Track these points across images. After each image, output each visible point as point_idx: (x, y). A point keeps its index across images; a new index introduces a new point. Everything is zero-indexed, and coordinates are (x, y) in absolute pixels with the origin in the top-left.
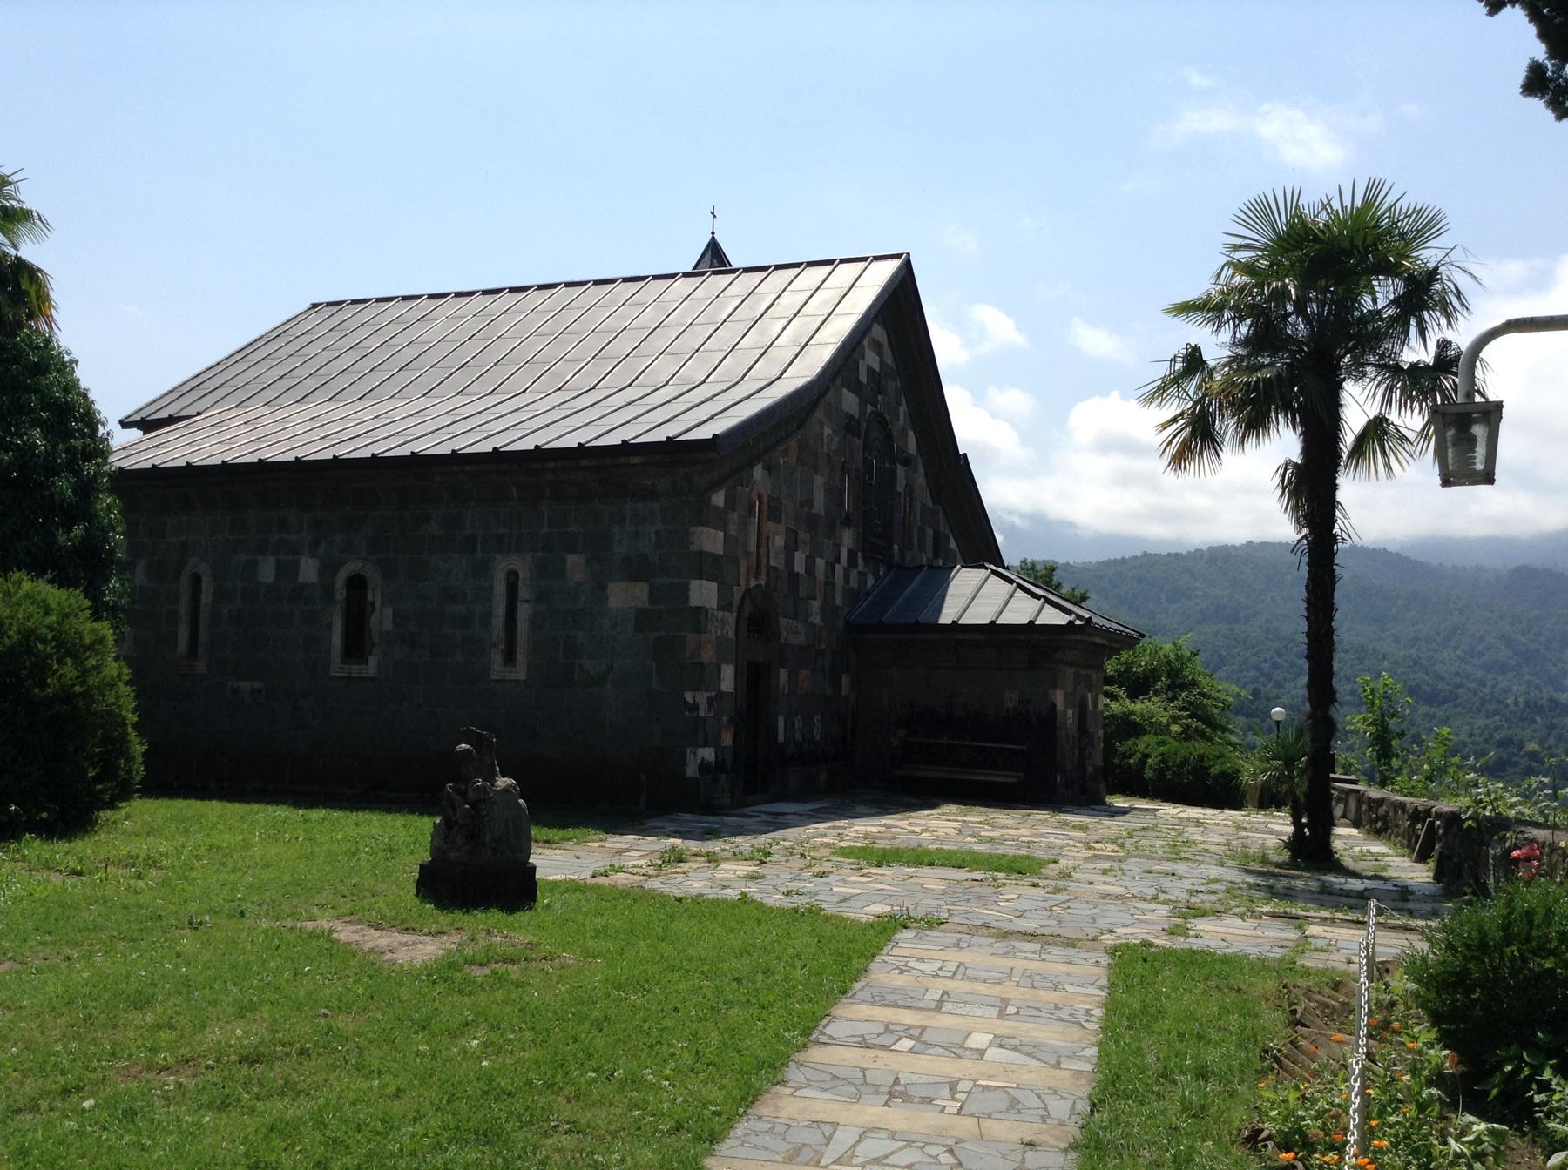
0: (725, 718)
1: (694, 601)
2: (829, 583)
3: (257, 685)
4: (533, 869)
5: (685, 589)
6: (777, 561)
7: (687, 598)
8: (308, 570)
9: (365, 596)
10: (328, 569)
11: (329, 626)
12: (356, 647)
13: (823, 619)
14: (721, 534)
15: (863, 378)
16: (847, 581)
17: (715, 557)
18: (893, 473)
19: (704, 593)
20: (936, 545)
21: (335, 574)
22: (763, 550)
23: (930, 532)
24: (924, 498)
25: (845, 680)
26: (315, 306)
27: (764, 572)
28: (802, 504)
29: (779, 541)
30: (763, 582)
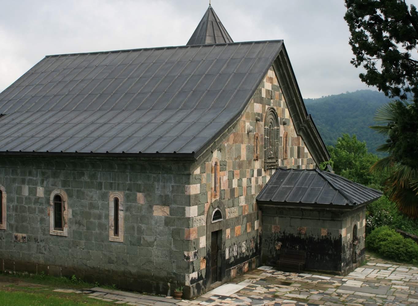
1: (187, 215)
2: (249, 187)
3: (24, 235)
5: (184, 209)
6: (224, 186)
7: (184, 214)
8: (40, 192)
10: (48, 192)
11: (49, 215)
12: (59, 224)
13: (246, 203)
16: (257, 182)
17: (196, 196)
18: (278, 130)
19: (192, 211)
21: (50, 195)
22: (218, 185)
23: (296, 148)
25: (256, 224)
27: (218, 194)
28: (236, 159)
29: (225, 178)
30: (218, 198)
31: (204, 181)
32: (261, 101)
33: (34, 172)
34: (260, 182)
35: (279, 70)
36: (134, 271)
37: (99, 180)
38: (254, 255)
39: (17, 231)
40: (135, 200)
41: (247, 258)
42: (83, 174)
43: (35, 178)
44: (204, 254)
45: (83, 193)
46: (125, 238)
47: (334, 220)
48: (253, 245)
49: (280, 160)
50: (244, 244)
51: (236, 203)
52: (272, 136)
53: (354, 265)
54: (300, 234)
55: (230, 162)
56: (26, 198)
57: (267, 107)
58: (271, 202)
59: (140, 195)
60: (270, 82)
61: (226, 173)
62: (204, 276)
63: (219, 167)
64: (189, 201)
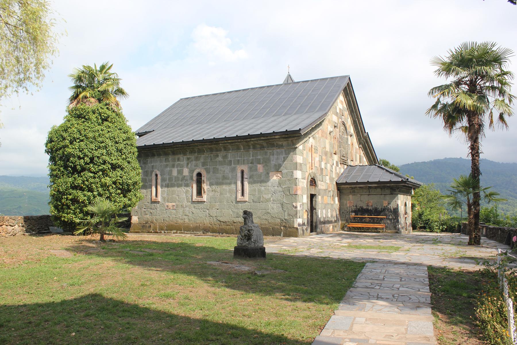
0: (304, 210)
1: (295, 177)
3: (174, 204)
4: (265, 248)
6: (317, 165)
7: (292, 176)
8: (186, 172)
9: (201, 179)
10: (191, 172)
14: (302, 157)
15: (338, 111)
16: (336, 170)
17: (301, 164)
19: (298, 174)
20: (360, 159)
21: (193, 173)
22: (313, 162)
24: (356, 145)
26: (181, 99)
28: (323, 148)
29: (317, 159)
31: (305, 156)
33: (181, 158)
35: (346, 97)
37: (229, 159)
38: (335, 221)
39: (168, 201)
42: (218, 156)
43: (182, 163)
45: (218, 169)
46: (249, 198)
47: (392, 194)
48: (334, 214)
52: (342, 143)
54: (368, 206)
56: (175, 177)
57: (340, 120)
58: (346, 183)
59: (260, 167)
60: (341, 103)
61: (318, 155)
62: (306, 224)
63: (313, 149)
64: (296, 166)
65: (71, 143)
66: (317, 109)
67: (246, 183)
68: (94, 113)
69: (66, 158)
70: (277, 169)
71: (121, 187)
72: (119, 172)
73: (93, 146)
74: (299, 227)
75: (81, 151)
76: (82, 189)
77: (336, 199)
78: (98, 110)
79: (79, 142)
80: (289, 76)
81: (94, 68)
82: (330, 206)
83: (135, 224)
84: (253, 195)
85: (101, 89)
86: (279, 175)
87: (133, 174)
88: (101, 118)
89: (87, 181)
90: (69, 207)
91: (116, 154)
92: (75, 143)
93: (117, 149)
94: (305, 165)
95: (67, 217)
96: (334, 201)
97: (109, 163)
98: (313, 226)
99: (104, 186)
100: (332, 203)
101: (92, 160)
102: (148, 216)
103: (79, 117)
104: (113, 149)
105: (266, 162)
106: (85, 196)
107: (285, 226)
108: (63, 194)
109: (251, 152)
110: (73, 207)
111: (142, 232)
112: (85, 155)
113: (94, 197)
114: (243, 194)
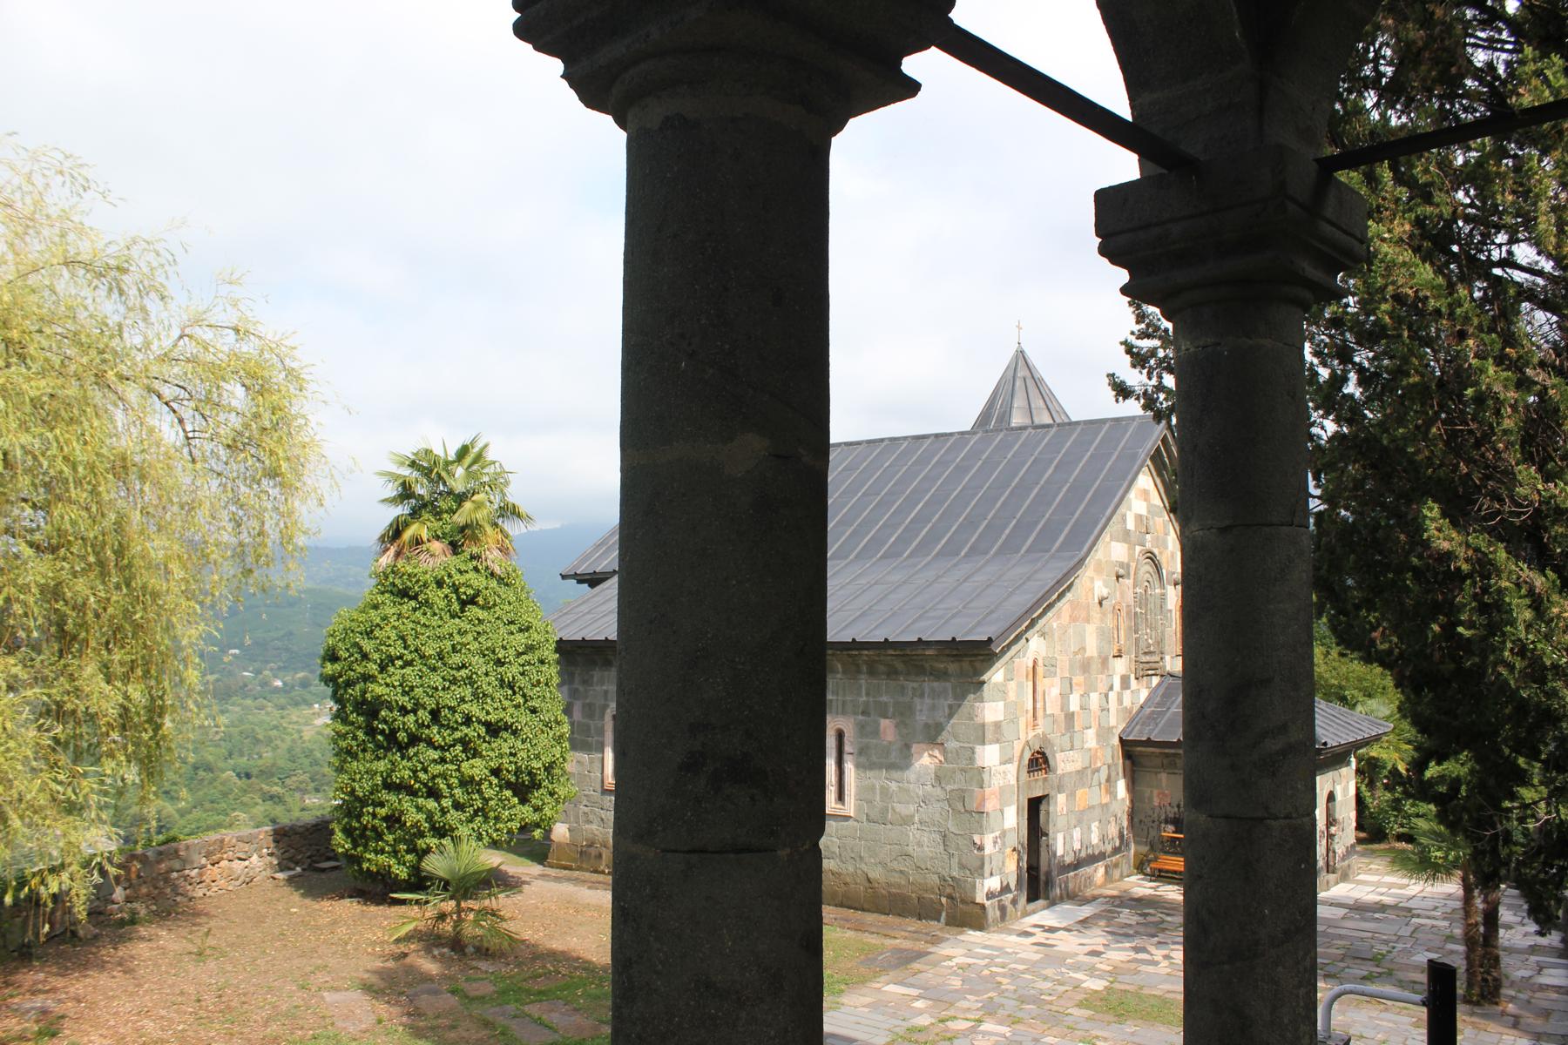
0: (1008, 850)
1: (979, 763)
6: (1053, 707)
7: (972, 759)
13: (1098, 742)
16: (1120, 701)
17: (997, 725)
18: (1163, 597)
19: (989, 755)
22: (1039, 705)
28: (1076, 653)
29: (1054, 692)
31: (1012, 696)
32: (1126, 536)
34: (1127, 702)
35: (1160, 475)
36: (876, 874)
38: (1116, 851)
40: (876, 733)
41: (1102, 856)
44: (1012, 841)
46: (858, 809)
48: (1113, 831)
49: (1167, 658)
50: (1095, 826)
51: (1077, 744)
53: (1332, 877)
55: (1063, 661)
57: (1138, 548)
58: (1149, 743)
59: (885, 724)
61: (1057, 680)
62: (1013, 886)
63: (1040, 670)
64: (981, 735)
65: (383, 669)
66: (1057, 544)
67: (849, 767)
68: (440, 584)
69: (371, 709)
70: (932, 735)
71: (513, 779)
72: (505, 743)
73: (436, 680)
74: (987, 903)
75: (405, 693)
76: (413, 793)
77: (1121, 787)
78: (450, 576)
79: (402, 667)
80: (1021, 356)
81: (442, 455)
82: (1097, 811)
83: (559, 845)
84: (869, 802)
85: (460, 518)
86: (936, 753)
87: (544, 740)
88: (458, 598)
89: (425, 770)
90: (379, 836)
91: (497, 695)
92: (391, 669)
93: (502, 680)
94: (1014, 721)
95: (374, 860)
96: (1111, 792)
97: (479, 722)
98: (1038, 882)
99: (467, 783)
100: (1106, 800)
101: (435, 714)
102: (594, 827)
103: (404, 594)
104: (488, 684)
105: (902, 714)
106: (419, 809)
107: (950, 897)
108: (363, 802)
109: (863, 681)
110: (390, 838)
111: (579, 869)
112: (418, 706)
113: (444, 812)
114: (841, 797)
